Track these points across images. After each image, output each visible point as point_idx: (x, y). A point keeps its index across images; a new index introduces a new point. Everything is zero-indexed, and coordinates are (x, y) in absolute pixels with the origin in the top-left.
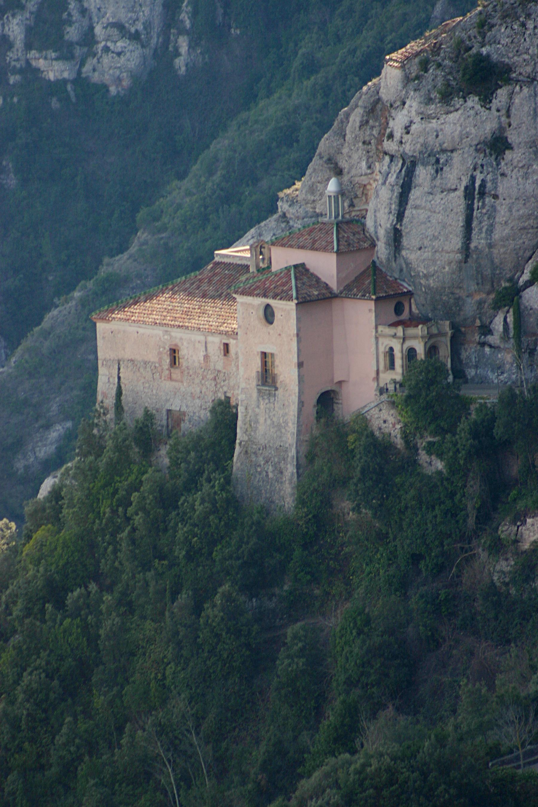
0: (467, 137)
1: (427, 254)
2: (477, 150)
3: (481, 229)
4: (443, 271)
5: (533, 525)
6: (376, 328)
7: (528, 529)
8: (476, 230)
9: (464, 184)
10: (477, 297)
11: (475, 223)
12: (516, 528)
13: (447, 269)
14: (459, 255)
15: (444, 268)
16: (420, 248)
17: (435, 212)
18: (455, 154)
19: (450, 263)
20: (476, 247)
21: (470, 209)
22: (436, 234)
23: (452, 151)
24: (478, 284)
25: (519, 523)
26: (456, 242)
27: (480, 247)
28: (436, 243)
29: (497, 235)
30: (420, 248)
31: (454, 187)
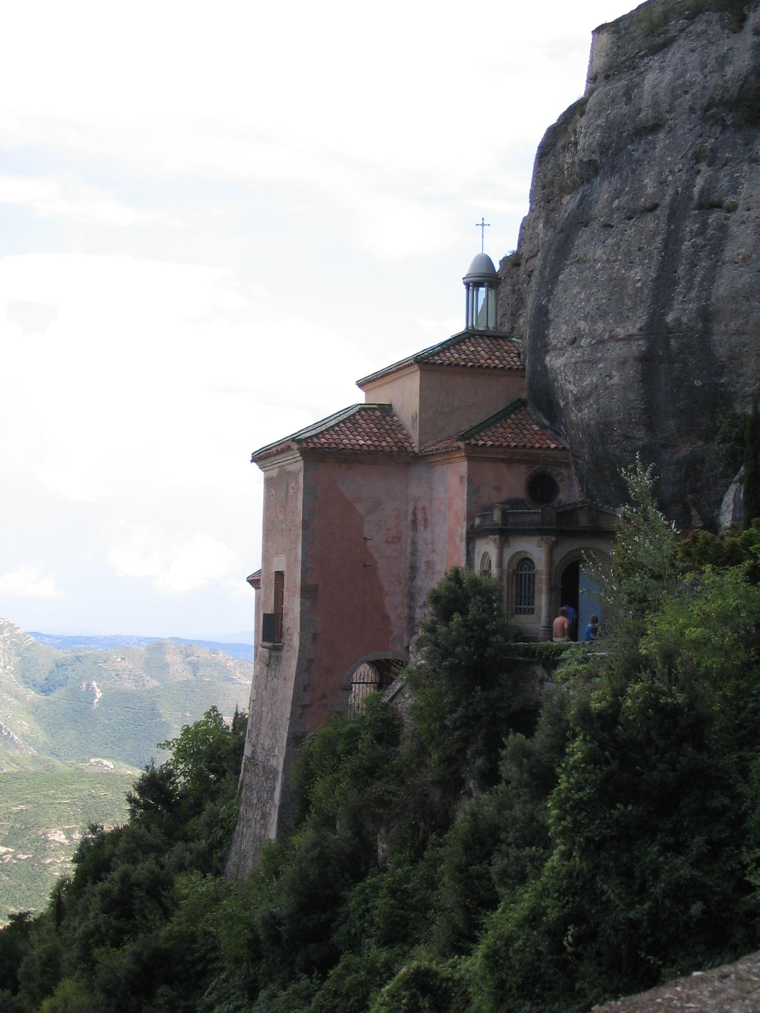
0: (686, 92)
2: (704, 119)
3: (691, 281)
4: (609, 383)
13: (616, 380)
14: (641, 342)
15: (611, 377)
16: (573, 342)
18: (661, 135)
19: (623, 363)
20: (678, 320)
21: (671, 241)
23: (656, 127)
27: (684, 320)
28: (600, 326)
29: (721, 289)
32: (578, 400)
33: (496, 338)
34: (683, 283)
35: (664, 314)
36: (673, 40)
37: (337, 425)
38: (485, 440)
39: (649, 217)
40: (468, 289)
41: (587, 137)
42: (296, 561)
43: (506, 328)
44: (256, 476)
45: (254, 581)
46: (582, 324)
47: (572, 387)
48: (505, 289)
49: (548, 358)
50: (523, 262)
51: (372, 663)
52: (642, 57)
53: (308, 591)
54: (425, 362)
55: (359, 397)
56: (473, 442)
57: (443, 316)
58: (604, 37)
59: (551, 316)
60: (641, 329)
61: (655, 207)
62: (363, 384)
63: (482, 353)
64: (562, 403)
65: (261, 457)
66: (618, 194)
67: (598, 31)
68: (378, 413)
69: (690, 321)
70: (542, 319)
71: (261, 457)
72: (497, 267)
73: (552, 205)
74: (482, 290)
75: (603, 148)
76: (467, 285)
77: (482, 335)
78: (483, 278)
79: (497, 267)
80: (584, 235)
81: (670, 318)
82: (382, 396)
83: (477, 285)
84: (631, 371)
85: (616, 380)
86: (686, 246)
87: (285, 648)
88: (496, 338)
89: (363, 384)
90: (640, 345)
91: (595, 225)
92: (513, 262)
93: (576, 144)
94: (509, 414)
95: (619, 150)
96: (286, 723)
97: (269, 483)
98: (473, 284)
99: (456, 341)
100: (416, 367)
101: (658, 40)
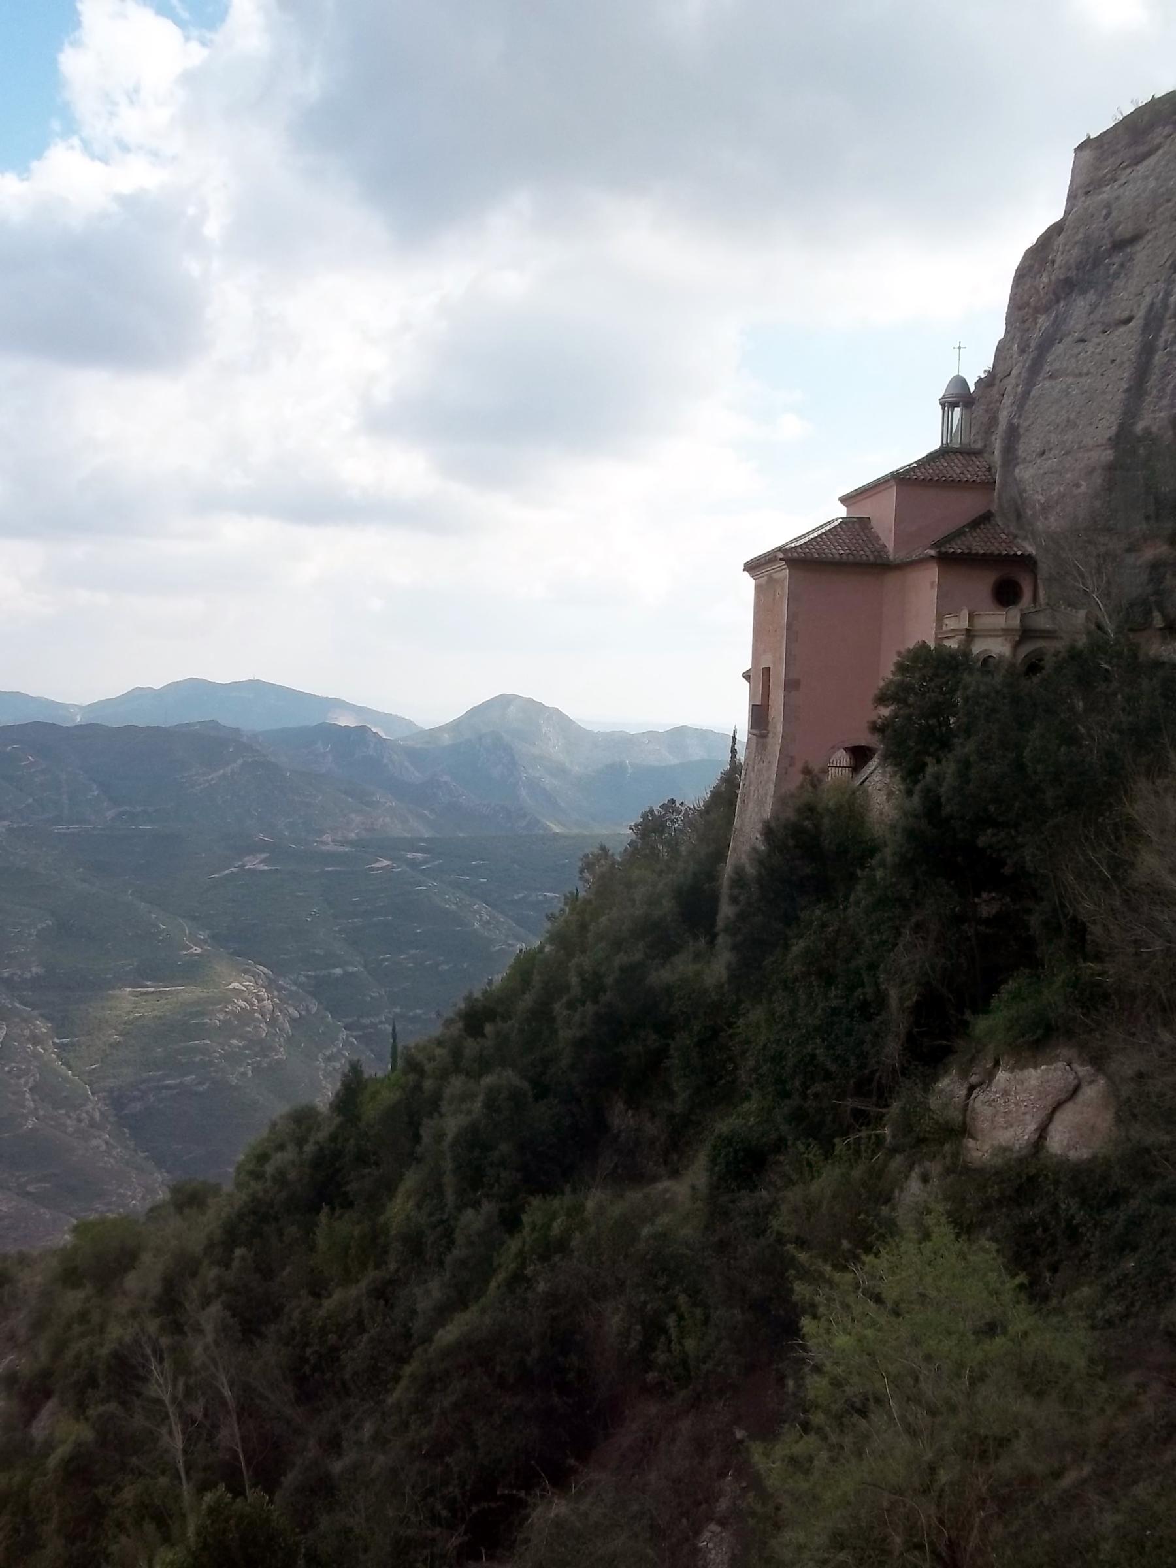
0: (1169, 201)
1: (1049, 463)
4: (1076, 492)
5: (1006, 1093)
6: (939, 620)
7: (990, 1103)
8: (1155, 392)
9: (1148, 299)
10: (1149, 554)
11: (1153, 379)
12: (964, 1092)
13: (1083, 489)
14: (1109, 452)
15: (1078, 486)
17: (1080, 375)
18: (1138, 247)
21: (1147, 350)
22: (1072, 416)
23: (1135, 239)
24: (1147, 518)
25: (974, 1079)
26: (1107, 425)
27: (1154, 429)
30: (1043, 453)
31: (1126, 314)
32: (1046, 509)
33: (968, 454)
34: (1155, 392)
35: (1133, 424)
36: (1159, 147)
37: (819, 536)
38: (956, 548)
39: (1122, 329)
40: (944, 409)
41: (1064, 256)
42: (781, 658)
43: (979, 446)
44: (748, 584)
45: (747, 676)
46: (1054, 438)
47: (1040, 497)
48: (979, 409)
49: (1017, 471)
50: (997, 381)
51: (846, 749)
52: (1125, 168)
53: (791, 685)
54: (903, 479)
55: (842, 512)
56: (943, 550)
57: (918, 435)
58: (1087, 154)
59: (1021, 431)
60: (1110, 439)
61: (1129, 320)
62: (844, 500)
63: (955, 468)
64: (1029, 512)
65: (752, 567)
66: (1094, 307)
67: (1079, 149)
68: (857, 526)
69: (1159, 429)
70: (1013, 433)
71: (752, 567)
72: (972, 389)
73: (1027, 325)
74: (957, 410)
75: (1080, 266)
76: (943, 405)
77: (956, 452)
78: (958, 398)
79: (972, 389)
80: (1059, 348)
81: (1139, 427)
82: (863, 511)
83: (953, 405)
84: (1098, 479)
85: (1083, 489)
86: (1159, 358)
87: (770, 735)
88: (968, 454)
89: (844, 500)
90: (1108, 455)
91: (1068, 340)
92: (988, 382)
93: (1053, 262)
94: (979, 524)
95: (1096, 264)
96: (770, 800)
97: (758, 589)
98: (947, 405)
99: (932, 457)
100: (893, 483)
101: (1143, 149)
